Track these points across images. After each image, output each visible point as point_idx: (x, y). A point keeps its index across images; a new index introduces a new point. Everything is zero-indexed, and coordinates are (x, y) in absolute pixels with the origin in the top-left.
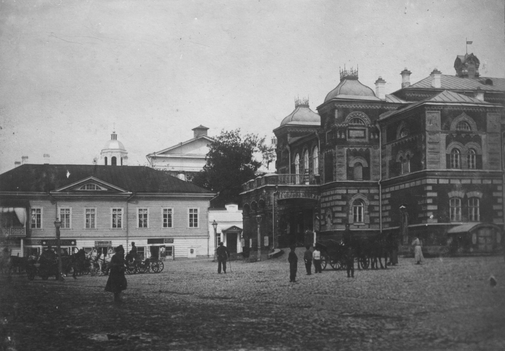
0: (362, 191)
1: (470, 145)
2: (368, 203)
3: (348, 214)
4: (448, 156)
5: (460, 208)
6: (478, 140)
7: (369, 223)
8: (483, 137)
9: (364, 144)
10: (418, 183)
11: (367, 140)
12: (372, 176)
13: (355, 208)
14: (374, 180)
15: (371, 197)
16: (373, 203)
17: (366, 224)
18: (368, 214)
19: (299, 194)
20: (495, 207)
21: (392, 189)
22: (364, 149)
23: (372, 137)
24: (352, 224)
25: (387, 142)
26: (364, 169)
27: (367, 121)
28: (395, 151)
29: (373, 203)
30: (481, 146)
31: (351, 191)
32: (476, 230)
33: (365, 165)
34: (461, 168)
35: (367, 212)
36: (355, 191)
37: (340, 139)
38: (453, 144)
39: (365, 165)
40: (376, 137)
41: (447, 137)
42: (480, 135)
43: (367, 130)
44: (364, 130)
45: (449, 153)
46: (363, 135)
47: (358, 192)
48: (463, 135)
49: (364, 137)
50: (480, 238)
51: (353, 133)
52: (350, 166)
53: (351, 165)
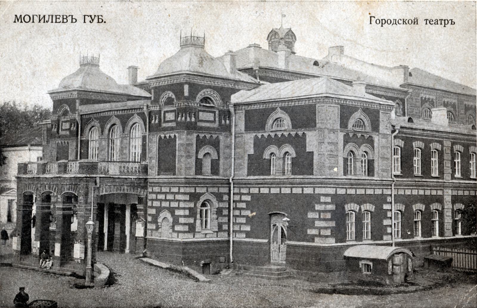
0: (210, 190)
1: (364, 148)
2: (216, 204)
3: (195, 220)
4: (346, 160)
5: (354, 223)
6: (370, 141)
7: (217, 230)
8: (376, 139)
9: (213, 129)
10: (308, 191)
11: (216, 125)
12: (221, 171)
13: (201, 211)
14: (224, 176)
15: (219, 197)
16: (222, 205)
17: (214, 232)
18: (217, 219)
19: (122, 188)
20: (386, 222)
21: (255, 191)
22: (215, 136)
23: (223, 122)
24: (199, 232)
25: (245, 131)
26: (212, 161)
27: (217, 100)
28: (260, 145)
29: (222, 205)
30: (373, 147)
31: (198, 190)
32: (392, 257)
33: (215, 156)
34: (355, 175)
35: (215, 216)
36: (204, 190)
37: (191, 122)
38: (350, 146)
39: (215, 156)
40: (228, 122)
41: (345, 136)
42: (373, 136)
43: (217, 112)
44: (214, 112)
45: (346, 157)
46: (212, 119)
47: (207, 190)
48: (359, 135)
49: (214, 121)
50: (394, 267)
51: (202, 116)
52: (199, 157)
53: (200, 156)
